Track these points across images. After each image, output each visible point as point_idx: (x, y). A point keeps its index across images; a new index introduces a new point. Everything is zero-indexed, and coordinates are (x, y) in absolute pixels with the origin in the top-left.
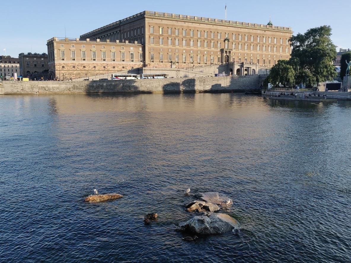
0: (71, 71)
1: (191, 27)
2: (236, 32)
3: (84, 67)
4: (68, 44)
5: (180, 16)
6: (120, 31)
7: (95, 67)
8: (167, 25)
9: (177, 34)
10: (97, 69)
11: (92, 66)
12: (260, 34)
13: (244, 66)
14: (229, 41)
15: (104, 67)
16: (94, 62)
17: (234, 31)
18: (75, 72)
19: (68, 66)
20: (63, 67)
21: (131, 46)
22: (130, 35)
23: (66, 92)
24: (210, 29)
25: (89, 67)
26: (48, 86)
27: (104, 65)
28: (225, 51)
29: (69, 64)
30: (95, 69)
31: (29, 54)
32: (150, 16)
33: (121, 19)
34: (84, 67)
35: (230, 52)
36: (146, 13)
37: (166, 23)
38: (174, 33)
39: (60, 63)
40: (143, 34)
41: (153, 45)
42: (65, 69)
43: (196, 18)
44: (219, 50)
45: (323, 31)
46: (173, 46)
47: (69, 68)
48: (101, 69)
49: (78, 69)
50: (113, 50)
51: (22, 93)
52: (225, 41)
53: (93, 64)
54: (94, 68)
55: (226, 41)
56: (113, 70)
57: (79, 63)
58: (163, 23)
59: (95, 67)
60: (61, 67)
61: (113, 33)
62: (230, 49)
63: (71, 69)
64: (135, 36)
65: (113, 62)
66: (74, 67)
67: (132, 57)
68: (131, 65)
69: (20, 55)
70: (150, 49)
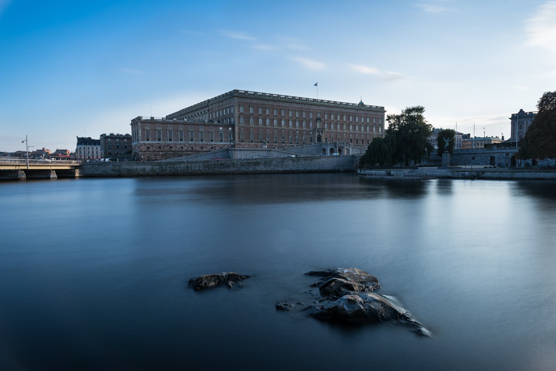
2: (329, 111)
6: (208, 110)
7: (182, 148)
8: (257, 104)
11: (178, 147)
12: (353, 113)
15: (192, 148)
16: (182, 142)
17: (326, 111)
18: (161, 153)
20: (148, 148)
21: (221, 126)
22: (219, 114)
24: (301, 108)
27: (191, 146)
31: (112, 134)
34: (171, 147)
35: (322, 131)
39: (144, 144)
45: (420, 109)
55: (318, 121)
59: (182, 148)
61: (201, 113)
64: (224, 116)
65: (201, 143)
66: (160, 147)
69: (101, 136)
70: (239, 129)
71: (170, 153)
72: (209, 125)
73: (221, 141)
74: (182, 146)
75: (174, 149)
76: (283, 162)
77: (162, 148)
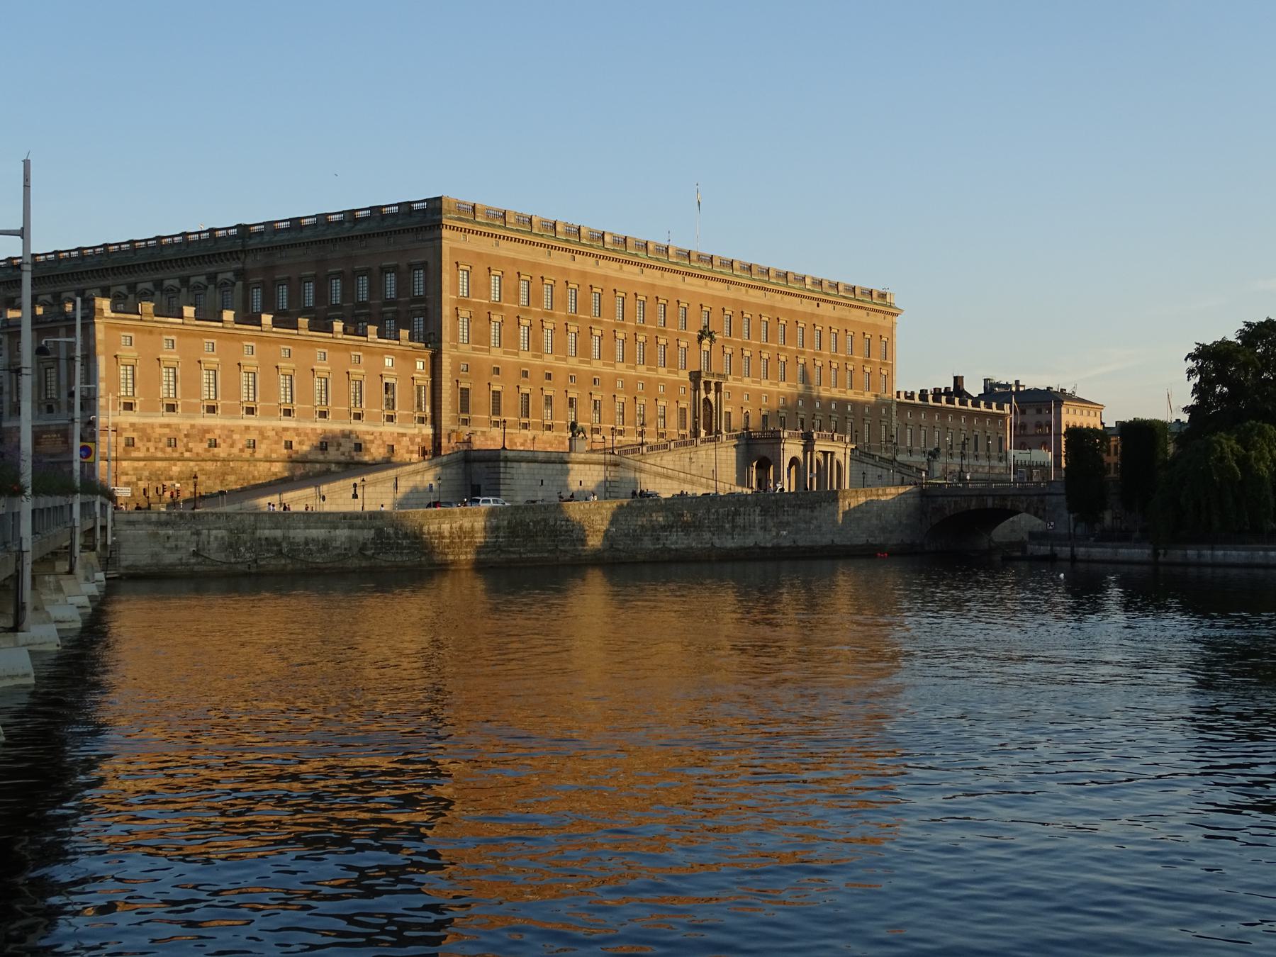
0: (159, 464)
1: (594, 276)
3: (214, 444)
4: (151, 332)
5: (558, 228)
6: (240, 274)
8: (514, 262)
9: (546, 304)
10: (261, 451)
13: (816, 448)
14: (712, 340)
15: (289, 445)
16: (251, 421)
19: (149, 440)
20: (130, 443)
21: (389, 352)
23: (353, 563)
24: (653, 286)
25: (232, 446)
26: (292, 533)
27: (288, 436)
28: (706, 383)
29: (152, 426)
30: (252, 455)
32: (460, 219)
33: (255, 215)
36: (445, 206)
37: (512, 255)
38: (539, 303)
40: (421, 299)
41: (466, 350)
42: (134, 454)
43: (607, 238)
44: (684, 376)
46: (535, 356)
47: (152, 450)
48: (274, 456)
49: (187, 455)
50: (322, 367)
51: (196, 568)
52: (700, 339)
53: (247, 428)
54: (251, 450)
55: (706, 341)
56: (321, 457)
57: (193, 426)
58: (503, 253)
59: (253, 445)
60: (122, 441)
62: (719, 375)
63: (159, 454)
67: (391, 404)
68: (385, 439)
70: (455, 369)
71: (210, 466)
72: (347, 348)
73: (391, 419)
74: (254, 435)
75: (221, 452)
76: (737, 513)
77: (180, 448)
